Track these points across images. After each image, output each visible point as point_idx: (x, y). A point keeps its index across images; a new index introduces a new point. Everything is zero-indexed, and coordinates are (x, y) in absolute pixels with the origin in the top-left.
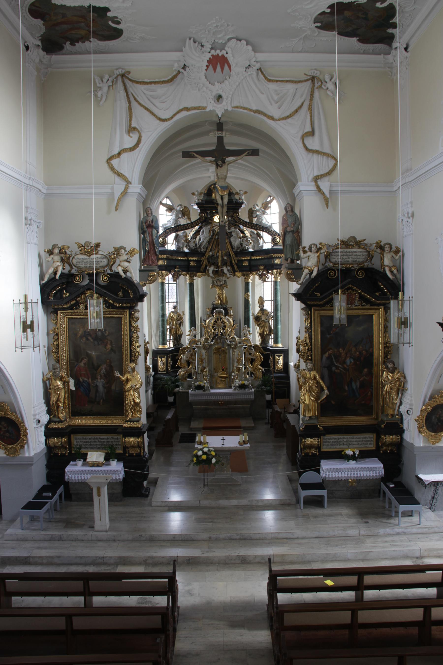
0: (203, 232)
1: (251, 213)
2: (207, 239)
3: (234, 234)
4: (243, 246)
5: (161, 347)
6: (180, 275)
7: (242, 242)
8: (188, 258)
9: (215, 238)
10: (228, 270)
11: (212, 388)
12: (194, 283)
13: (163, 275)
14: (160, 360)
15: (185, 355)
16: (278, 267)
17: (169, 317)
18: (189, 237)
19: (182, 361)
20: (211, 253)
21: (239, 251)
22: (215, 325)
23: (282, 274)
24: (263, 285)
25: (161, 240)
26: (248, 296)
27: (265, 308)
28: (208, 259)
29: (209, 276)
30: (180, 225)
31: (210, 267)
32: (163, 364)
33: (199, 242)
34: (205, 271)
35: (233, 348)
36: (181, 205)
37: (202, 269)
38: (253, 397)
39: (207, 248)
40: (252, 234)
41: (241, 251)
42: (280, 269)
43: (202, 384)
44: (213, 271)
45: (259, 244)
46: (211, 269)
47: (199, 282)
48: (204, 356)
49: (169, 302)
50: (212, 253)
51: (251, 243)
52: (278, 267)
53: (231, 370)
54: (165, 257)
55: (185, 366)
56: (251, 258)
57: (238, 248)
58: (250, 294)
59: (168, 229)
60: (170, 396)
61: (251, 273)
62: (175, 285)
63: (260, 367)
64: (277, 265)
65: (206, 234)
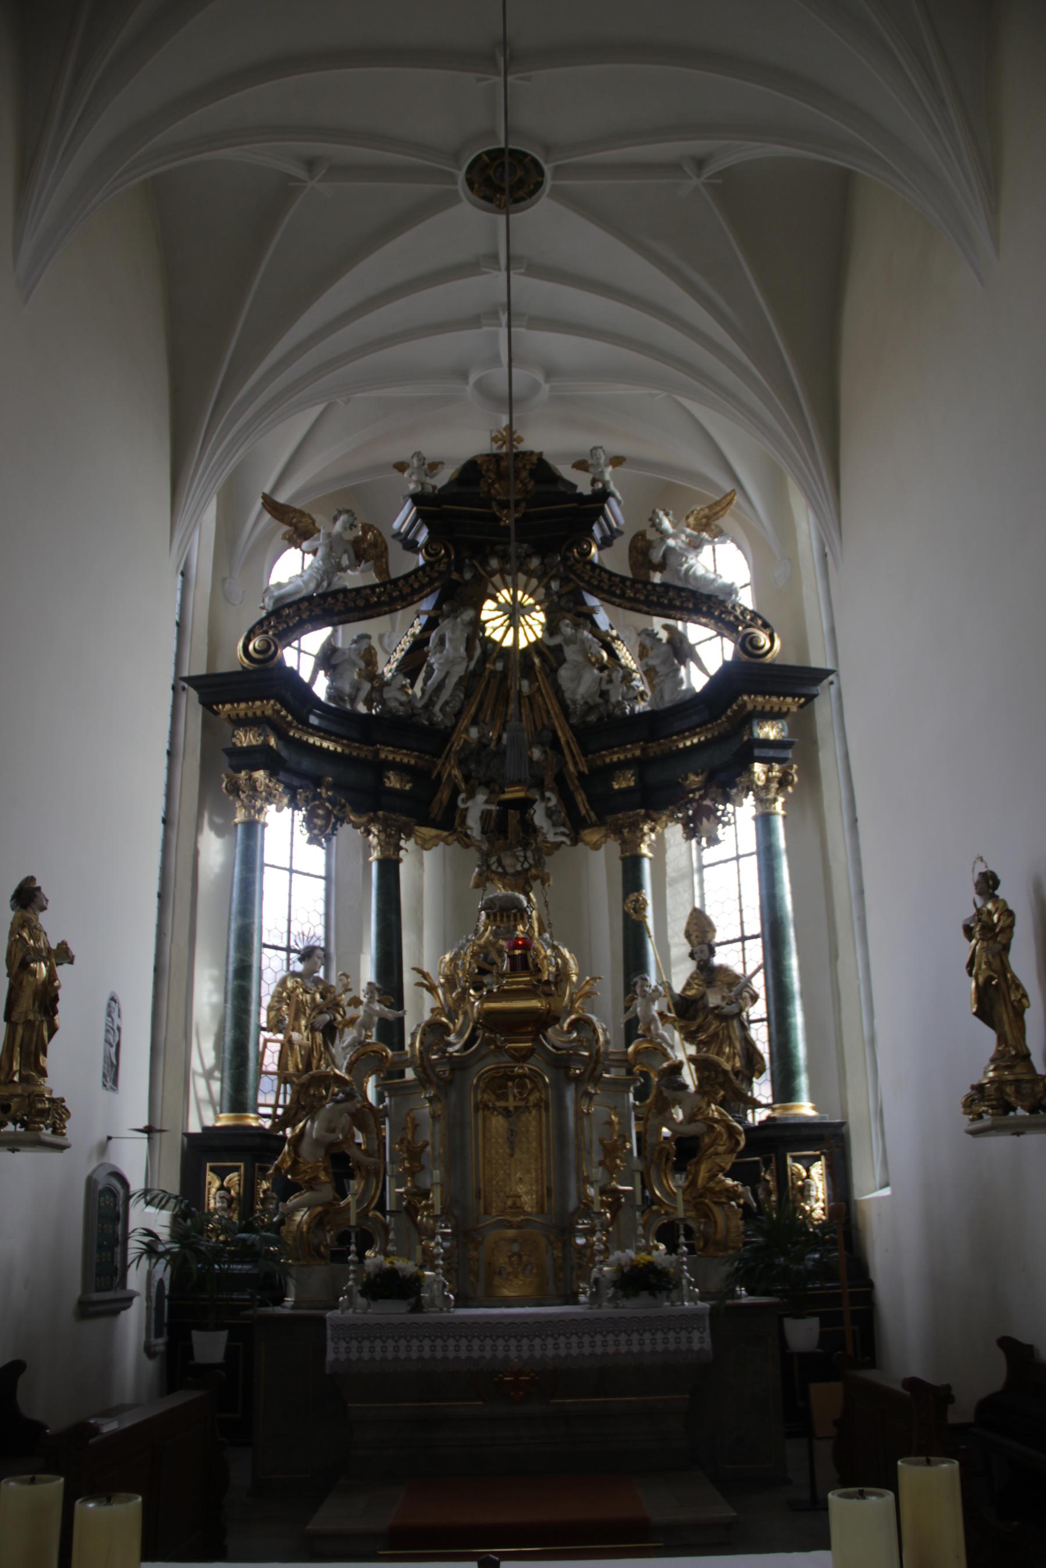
0: (442, 641)
1: (642, 551)
2: (459, 670)
3: (570, 653)
4: (613, 700)
5: (225, 1120)
6: (341, 820)
7: (605, 687)
8: (377, 753)
9: (493, 673)
10: (549, 814)
11: (463, 1301)
12: (402, 867)
13: (254, 789)
14: (217, 1183)
15: (322, 1114)
16: (771, 753)
17: (278, 997)
18: (387, 670)
19: (305, 1147)
20: (474, 733)
21: (592, 718)
22: (486, 979)
23: (791, 783)
24: (701, 882)
25: (255, 644)
26: (639, 907)
27: (717, 960)
28: (462, 763)
29: (465, 840)
30: (345, 591)
31: (471, 795)
32: (230, 1201)
33: (423, 691)
34: (449, 822)
35: (577, 1079)
36: (347, 512)
37: (436, 810)
38: (708, 1344)
39: (458, 715)
40: (648, 642)
41: (600, 719)
42: (780, 761)
43: (406, 1266)
44: (485, 816)
45: (681, 682)
46: (476, 808)
47: (422, 869)
48: (426, 1134)
49: (288, 950)
50: (482, 735)
51: (642, 694)
52: (771, 753)
53: (572, 1204)
54: (269, 712)
55: (316, 1178)
56: (644, 750)
57: (590, 708)
58: (647, 892)
59: (289, 605)
60: (204, 1328)
61: (647, 817)
62: (322, 883)
63: (729, 1182)
64: (766, 743)
65: (456, 649)
